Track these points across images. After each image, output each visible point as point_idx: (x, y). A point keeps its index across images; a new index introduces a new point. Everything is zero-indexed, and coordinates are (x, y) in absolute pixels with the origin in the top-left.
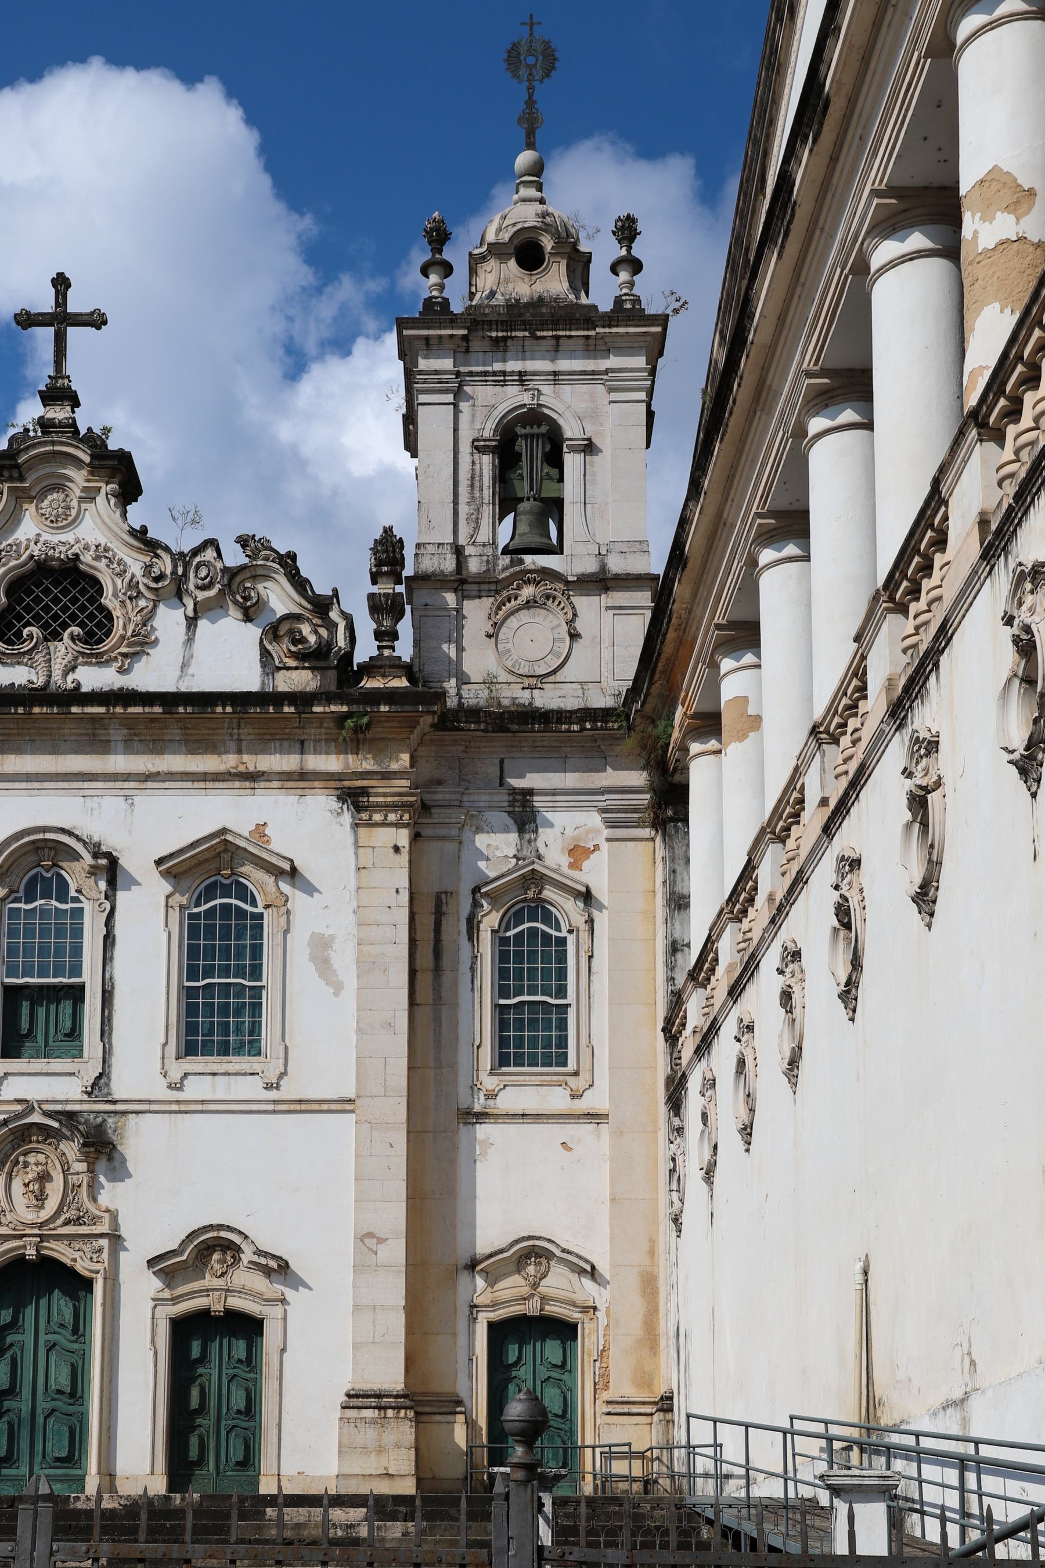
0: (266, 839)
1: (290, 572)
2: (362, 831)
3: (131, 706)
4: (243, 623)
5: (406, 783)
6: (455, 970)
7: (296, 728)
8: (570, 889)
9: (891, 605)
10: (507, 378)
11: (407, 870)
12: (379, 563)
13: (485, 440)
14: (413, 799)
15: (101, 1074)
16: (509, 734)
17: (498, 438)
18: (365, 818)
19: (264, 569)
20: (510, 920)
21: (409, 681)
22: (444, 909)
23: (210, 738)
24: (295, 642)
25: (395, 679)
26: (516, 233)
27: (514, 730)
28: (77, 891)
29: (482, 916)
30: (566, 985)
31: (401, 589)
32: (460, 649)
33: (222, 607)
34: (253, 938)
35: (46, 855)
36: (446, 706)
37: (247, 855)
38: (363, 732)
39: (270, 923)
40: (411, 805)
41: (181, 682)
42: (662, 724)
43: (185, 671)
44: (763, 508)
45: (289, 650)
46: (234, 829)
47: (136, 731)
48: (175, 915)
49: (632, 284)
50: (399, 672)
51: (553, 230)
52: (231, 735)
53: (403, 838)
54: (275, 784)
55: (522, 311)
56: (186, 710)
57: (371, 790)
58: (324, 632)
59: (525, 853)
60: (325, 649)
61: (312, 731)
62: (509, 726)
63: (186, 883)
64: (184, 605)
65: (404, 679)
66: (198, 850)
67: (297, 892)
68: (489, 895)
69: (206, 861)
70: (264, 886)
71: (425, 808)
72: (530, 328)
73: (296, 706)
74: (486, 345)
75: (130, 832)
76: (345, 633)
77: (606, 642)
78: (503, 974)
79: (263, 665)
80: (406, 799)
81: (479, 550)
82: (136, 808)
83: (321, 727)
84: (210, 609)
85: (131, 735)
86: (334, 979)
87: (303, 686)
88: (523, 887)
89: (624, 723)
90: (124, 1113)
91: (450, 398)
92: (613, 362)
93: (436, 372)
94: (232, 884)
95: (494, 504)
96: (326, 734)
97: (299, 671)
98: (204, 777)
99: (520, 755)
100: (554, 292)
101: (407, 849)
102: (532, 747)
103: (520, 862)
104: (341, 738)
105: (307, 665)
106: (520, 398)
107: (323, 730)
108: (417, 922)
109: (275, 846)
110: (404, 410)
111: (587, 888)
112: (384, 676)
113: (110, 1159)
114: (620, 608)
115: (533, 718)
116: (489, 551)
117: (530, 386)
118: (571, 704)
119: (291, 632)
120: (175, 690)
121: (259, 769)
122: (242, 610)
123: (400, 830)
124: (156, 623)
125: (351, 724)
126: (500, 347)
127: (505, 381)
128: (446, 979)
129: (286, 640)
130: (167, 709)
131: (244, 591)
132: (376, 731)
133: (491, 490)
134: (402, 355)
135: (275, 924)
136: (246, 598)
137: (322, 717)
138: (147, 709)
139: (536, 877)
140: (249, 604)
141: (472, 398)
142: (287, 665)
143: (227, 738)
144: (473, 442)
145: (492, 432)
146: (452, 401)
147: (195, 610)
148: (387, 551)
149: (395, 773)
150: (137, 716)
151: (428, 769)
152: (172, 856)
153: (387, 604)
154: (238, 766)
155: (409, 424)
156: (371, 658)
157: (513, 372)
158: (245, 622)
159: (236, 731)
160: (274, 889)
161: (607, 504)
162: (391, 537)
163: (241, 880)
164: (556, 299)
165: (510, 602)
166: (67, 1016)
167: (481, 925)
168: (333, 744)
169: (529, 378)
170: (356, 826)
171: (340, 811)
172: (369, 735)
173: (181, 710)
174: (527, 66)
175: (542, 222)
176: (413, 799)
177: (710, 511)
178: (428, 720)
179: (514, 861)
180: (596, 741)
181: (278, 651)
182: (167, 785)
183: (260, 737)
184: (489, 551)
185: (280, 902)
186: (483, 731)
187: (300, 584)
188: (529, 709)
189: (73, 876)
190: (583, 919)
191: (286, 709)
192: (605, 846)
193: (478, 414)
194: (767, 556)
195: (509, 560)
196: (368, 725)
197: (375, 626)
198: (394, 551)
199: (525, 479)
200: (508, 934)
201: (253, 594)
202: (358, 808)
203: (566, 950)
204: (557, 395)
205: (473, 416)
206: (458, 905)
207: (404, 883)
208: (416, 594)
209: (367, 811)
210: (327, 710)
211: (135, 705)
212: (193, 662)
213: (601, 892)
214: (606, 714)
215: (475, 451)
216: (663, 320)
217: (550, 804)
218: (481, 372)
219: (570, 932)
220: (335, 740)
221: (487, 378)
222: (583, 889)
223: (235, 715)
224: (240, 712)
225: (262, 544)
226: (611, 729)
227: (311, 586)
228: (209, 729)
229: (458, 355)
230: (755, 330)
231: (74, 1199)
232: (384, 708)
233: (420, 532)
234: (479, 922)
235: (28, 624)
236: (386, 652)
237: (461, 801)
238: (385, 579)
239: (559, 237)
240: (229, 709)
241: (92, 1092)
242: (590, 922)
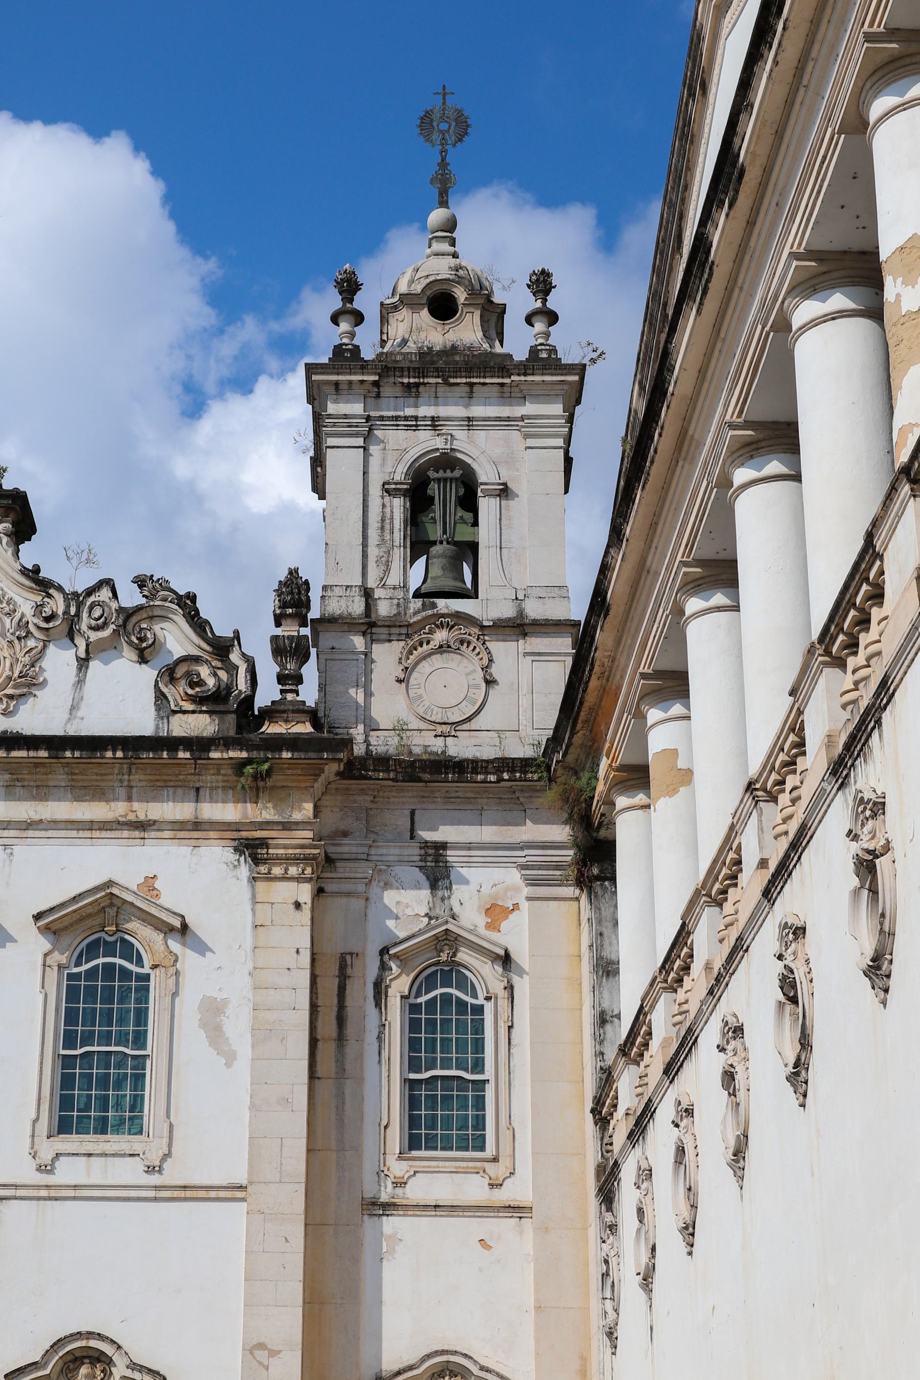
0: (155, 892)
1: (190, 613)
2: (261, 886)
3: (14, 750)
4: (138, 665)
5: (310, 834)
6: (360, 1040)
8: (487, 952)
9: (827, 659)
10: (419, 423)
11: (309, 928)
12: (284, 605)
13: (396, 484)
14: (316, 851)
16: (421, 784)
17: (410, 481)
18: (264, 872)
19: (161, 609)
20: (421, 983)
21: (314, 727)
22: (349, 971)
23: (98, 784)
24: (192, 685)
25: (299, 725)
26: (428, 284)
27: (426, 779)
29: (391, 980)
30: (483, 1058)
31: (306, 631)
32: (368, 694)
34: (138, 1001)
36: (352, 754)
37: (134, 910)
38: (263, 780)
40: (314, 858)
41: (69, 726)
42: (585, 776)
43: (74, 713)
44: (688, 557)
45: (186, 693)
46: (121, 882)
47: (19, 776)
48: (53, 975)
49: (547, 335)
50: (302, 717)
51: (467, 283)
52: (121, 781)
53: (305, 893)
54: (167, 834)
55: (435, 359)
57: (270, 841)
58: (223, 675)
59: (438, 911)
60: (225, 692)
61: (209, 778)
62: (421, 775)
63: (66, 940)
64: (76, 646)
65: (308, 724)
66: (81, 904)
67: (188, 952)
68: (398, 957)
69: (89, 916)
70: (151, 944)
71: (330, 861)
72: (443, 375)
73: (191, 751)
74: (398, 390)
75: (7, 884)
76: (246, 676)
77: (524, 690)
78: (414, 1044)
79: (158, 708)
80: (308, 851)
81: (390, 593)
82: (15, 859)
83: (218, 774)
84: (104, 650)
85: (13, 780)
87: (200, 730)
88: (436, 948)
89: (545, 774)
91: (360, 441)
92: (529, 408)
93: (346, 416)
94: (117, 941)
95: (405, 547)
96: (223, 781)
97: (196, 715)
98: (91, 826)
99: (432, 806)
100: (468, 341)
101: (309, 905)
102: (446, 798)
103: (432, 922)
104: (240, 786)
105: (204, 708)
106: (432, 443)
107: (220, 778)
108: (319, 985)
109: (166, 900)
110: (312, 453)
111: (506, 951)
112: (286, 721)
114: (539, 654)
115: (447, 767)
116: (400, 594)
117: (443, 432)
118: (487, 753)
119: (188, 674)
120: (61, 733)
121: (150, 817)
122: (137, 652)
123: (301, 885)
124: (45, 663)
125: (251, 771)
126: (412, 391)
127: (417, 426)
128: (351, 1050)
129: (183, 682)
130: (53, 753)
131: (140, 632)
132: (277, 779)
133: (402, 533)
134: (311, 399)
135: (163, 986)
136: (141, 640)
137: (219, 765)
138: (32, 754)
139: (449, 938)
140: (144, 645)
141: (383, 442)
142: (183, 709)
143: (117, 784)
144: (384, 485)
145: (403, 475)
146: (362, 444)
147: (87, 651)
148: (292, 593)
149: (297, 823)
150: (21, 760)
151: (332, 819)
152: (52, 910)
153: (291, 647)
154: (127, 815)
155: (317, 466)
156: (273, 702)
157: (425, 417)
158: (140, 663)
159: (126, 777)
160: (162, 948)
161: (524, 548)
162: (297, 578)
163: (127, 937)
164: (469, 348)
165: (421, 646)
167: (389, 990)
168: (230, 792)
169: (441, 423)
171: (236, 863)
172: (269, 783)
173: (68, 754)
174: (440, 131)
175: (455, 275)
176: (316, 851)
177: (633, 558)
178: (334, 767)
179: (426, 920)
180: (514, 792)
181: (175, 694)
182: (50, 833)
183: (152, 784)
184: (400, 594)
185: (168, 962)
186: (393, 780)
187: (199, 625)
188: (442, 757)
190: (502, 985)
191: (181, 755)
192: (525, 905)
193: (389, 458)
194: (693, 604)
195: (421, 603)
196: (269, 772)
197: (278, 669)
198: (299, 593)
199: (438, 522)
200: (419, 1000)
201: (149, 635)
202: (257, 860)
203: (483, 1020)
204: (471, 441)
205: (384, 459)
206: (364, 967)
207: (305, 942)
208: (321, 635)
209: (265, 863)
210: (225, 756)
211: (19, 749)
212: (83, 705)
213: (522, 955)
214: (525, 764)
215: (385, 494)
216: (581, 369)
217: (465, 859)
218: (393, 417)
219: (488, 999)
220: (233, 788)
221: (398, 423)
222: (502, 953)
223: (126, 761)
224: (132, 757)
225: (161, 585)
226: (530, 781)
227: (211, 628)
228: (97, 774)
229: (369, 400)
230: (676, 382)
232: (286, 755)
233: (327, 574)
234: (387, 987)
236: (290, 697)
237: (368, 855)
238: (289, 621)
239: (473, 289)
240: (119, 754)
242: (510, 988)
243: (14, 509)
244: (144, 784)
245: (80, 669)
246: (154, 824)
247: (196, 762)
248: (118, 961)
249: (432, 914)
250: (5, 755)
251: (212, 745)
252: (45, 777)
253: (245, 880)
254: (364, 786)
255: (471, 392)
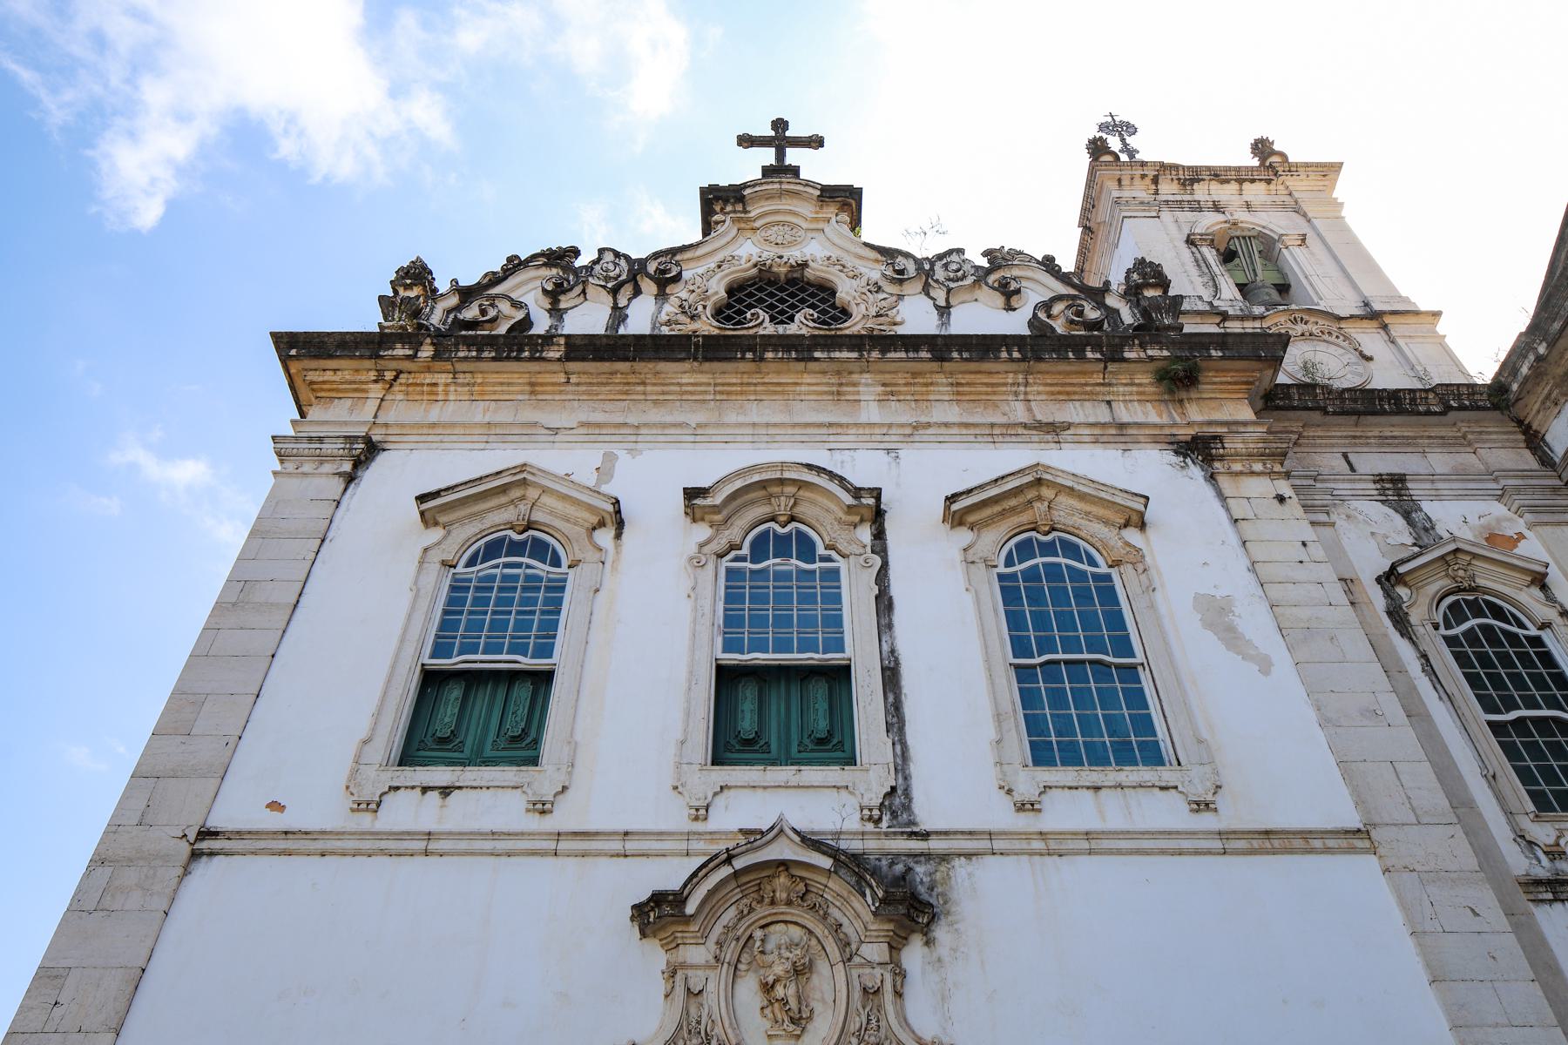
3: (890, 351)
7: (1102, 384)
15: (893, 789)
23: (989, 397)
28: (827, 547)
33: (976, 300)
35: (783, 504)
39: (1125, 584)
47: (894, 389)
52: (1016, 394)
56: (962, 355)
74: (1175, 187)
83: (1132, 384)
85: (886, 394)
86: (1252, 652)
90: (945, 858)
107: (1135, 389)
113: (929, 943)
147: (947, 300)
152: (969, 492)
159: (1022, 388)
160: (1120, 544)
166: (821, 713)
170: (1212, 478)
171: (1182, 464)
189: (821, 529)
211: (895, 351)
228: (987, 385)
231: (869, 1021)
235: (750, 307)
241: (880, 819)
243: (851, 205)
244: (1044, 397)
245: (941, 315)
246: (1069, 429)
247: (1105, 368)
248: (1061, 560)
249: (1420, 543)
250: (880, 356)
251: (1125, 346)
252: (924, 389)
253: (1202, 480)
254: (1286, 425)
255: (1241, 190)
